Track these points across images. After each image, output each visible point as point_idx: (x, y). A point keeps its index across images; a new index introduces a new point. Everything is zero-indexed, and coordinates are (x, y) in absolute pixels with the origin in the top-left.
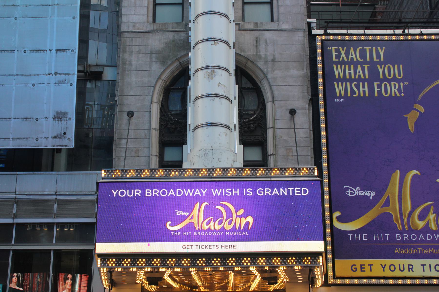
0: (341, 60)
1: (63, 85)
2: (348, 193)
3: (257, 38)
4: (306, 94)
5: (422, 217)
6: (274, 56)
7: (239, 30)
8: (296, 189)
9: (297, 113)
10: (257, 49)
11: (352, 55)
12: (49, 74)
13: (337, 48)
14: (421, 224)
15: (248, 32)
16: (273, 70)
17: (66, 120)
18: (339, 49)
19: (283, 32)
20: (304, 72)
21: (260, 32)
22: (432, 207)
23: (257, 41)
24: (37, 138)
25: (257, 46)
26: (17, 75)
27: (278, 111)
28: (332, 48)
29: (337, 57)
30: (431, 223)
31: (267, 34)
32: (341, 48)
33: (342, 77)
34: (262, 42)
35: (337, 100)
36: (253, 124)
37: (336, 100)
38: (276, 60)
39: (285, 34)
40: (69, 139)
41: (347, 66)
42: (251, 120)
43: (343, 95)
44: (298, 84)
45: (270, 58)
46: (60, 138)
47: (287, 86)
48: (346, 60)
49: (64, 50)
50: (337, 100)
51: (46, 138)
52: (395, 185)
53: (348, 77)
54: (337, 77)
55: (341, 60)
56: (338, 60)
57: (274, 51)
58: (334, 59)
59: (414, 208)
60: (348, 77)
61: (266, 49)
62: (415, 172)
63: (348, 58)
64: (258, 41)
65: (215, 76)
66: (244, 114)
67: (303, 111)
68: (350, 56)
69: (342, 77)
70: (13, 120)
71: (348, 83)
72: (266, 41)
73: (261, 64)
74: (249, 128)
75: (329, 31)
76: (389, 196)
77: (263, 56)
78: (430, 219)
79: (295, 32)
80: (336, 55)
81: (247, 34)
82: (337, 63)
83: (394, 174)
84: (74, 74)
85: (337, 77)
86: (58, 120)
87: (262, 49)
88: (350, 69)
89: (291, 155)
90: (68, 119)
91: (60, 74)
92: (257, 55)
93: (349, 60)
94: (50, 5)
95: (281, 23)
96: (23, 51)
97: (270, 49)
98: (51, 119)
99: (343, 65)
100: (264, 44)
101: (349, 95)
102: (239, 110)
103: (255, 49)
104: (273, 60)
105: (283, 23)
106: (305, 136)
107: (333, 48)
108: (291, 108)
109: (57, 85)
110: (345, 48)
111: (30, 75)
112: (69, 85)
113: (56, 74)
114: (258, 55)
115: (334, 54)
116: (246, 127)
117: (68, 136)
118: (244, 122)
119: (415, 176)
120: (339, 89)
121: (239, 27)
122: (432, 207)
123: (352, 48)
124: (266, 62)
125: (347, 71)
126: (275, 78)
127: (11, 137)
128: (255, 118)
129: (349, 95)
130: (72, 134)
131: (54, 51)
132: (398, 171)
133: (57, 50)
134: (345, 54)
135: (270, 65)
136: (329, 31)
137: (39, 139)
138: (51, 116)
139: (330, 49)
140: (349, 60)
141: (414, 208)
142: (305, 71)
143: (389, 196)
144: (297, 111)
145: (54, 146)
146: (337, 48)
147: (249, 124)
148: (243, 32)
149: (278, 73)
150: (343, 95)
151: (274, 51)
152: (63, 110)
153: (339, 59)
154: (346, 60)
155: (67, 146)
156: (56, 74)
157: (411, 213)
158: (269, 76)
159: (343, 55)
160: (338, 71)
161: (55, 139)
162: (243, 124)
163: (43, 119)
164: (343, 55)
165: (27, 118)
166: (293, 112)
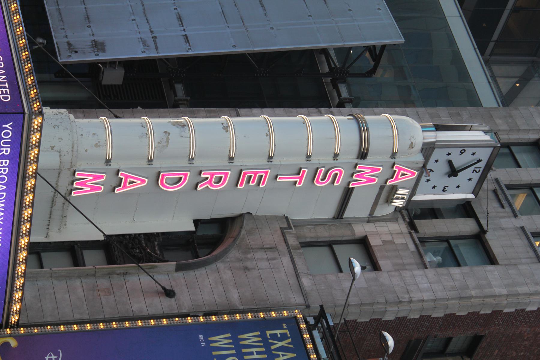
0: (270, 341)
1: (142, 45)
2: (50, 355)
3: (276, 248)
4: (204, 309)
6: (254, 269)
7: (281, 228)
8: (8, 90)
9: (168, 299)
10: (258, 248)
11: (283, 355)
12: (152, 32)
13: (289, 335)
15: (282, 238)
16: (230, 269)
17: (94, 52)
18: (288, 338)
19: (295, 278)
20: (238, 306)
21: (287, 252)
23: (270, 248)
24: (64, 29)
25: (262, 248)
26: (143, 5)
27: (167, 277)
28: (286, 329)
29: (274, 337)
31: (286, 260)
32: (290, 340)
33: (241, 343)
34: (270, 255)
35: (201, 337)
36: (141, 252)
37: (201, 336)
38: (247, 272)
39: (293, 281)
40: (69, 56)
41: (263, 349)
42: (145, 250)
43: (211, 345)
44: (217, 300)
45: (249, 264)
46: (69, 49)
47: (209, 286)
48: (273, 347)
49: (187, 41)
50: (201, 337)
51: (66, 37)
53: (244, 351)
54: (239, 337)
55: (270, 341)
56: (269, 337)
57: (262, 269)
58: (268, 333)
60: (244, 351)
61: (262, 259)
63: (276, 350)
64: (271, 250)
65: (177, 127)
66: (153, 242)
67: (176, 307)
68: (281, 353)
69: (241, 343)
70: (83, 7)
71: (234, 352)
72: (274, 259)
73: (234, 254)
74: (133, 248)
75: (316, 333)
77: (249, 256)
79: (301, 294)
80: (276, 334)
81: (277, 237)
82: (263, 335)
84: (158, 53)
85: (239, 337)
86: (92, 45)
87: (259, 255)
88: (258, 353)
89: (101, 294)
90: (97, 53)
91: (155, 41)
92: (249, 249)
93: (274, 352)
94: (244, 24)
95: (311, 277)
96: (175, 7)
97: (264, 264)
98: (93, 38)
99: (262, 344)
100: (269, 257)
101: (214, 353)
102: (157, 233)
103: (257, 247)
104: (246, 269)
105: (310, 279)
106: (134, 310)
107: (287, 331)
108: (176, 292)
109: (140, 40)
110: (293, 346)
111: (146, 16)
112: (143, 50)
113: (154, 38)
114: (248, 249)
115: (278, 332)
116: (132, 245)
117: (73, 55)
118: (140, 242)
120: (221, 340)
121: (285, 228)
123: (295, 355)
124: (241, 260)
125: (254, 350)
126: (218, 271)
127: (60, 7)
128: (150, 254)
129: (214, 353)
130: (76, 58)
131: (184, 33)
133: (186, 36)
134: (282, 346)
135: (237, 265)
136: (316, 333)
137: (63, 31)
138: (95, 38)
139: (285, 327)
140: (274, 352)
142: (241, 307)
144: (173, 299)
145: (57, 44)
146: (289, 335)
147: (138, 248)
148: (279, 232)
149: (227, 275)
150: (211, 345)
151: (262, 269)
152: (106, 48)
153: (270, 339)
154: (273, 347)
155: (60, 54)
156: (154, 38)
158: (220, 265)
159: (280, 344)
160: (250, 338)
161: (66, 44)
162: (137, 240)
163: (90, 32)
164: (280, 344)
165: (88, 18)
166: (169, 293)
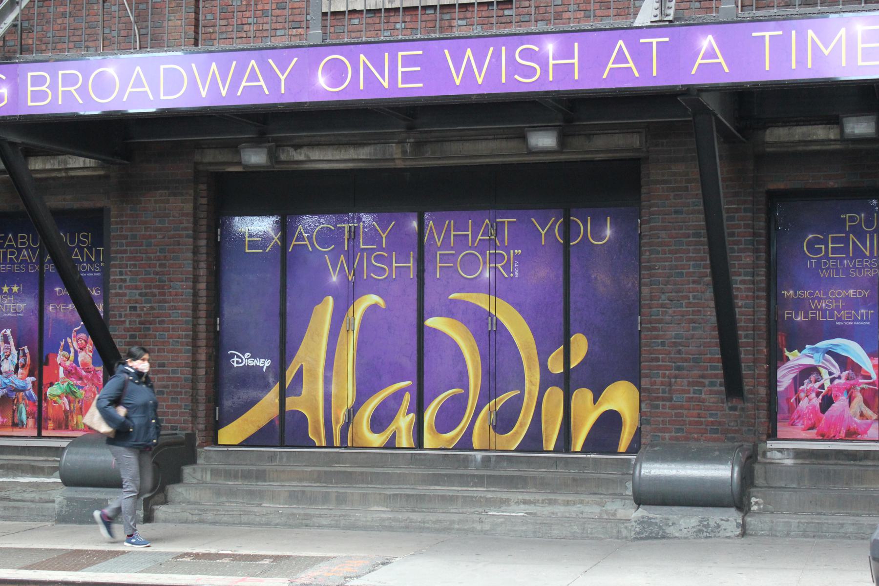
5: (379, 422)
14: (377, 440)
22: (407, 397)
30: (400, 437)
52: (320, 335)
59: (361, 398)
62: (372, 299)
76: (302, 366)
78: (399, 429)
83: (318, 307)
119: (374, 307)
122: (407, 397)
132: (330, 299)
141: (361, 398)
143: (302, 366)
157: (352, 413)
